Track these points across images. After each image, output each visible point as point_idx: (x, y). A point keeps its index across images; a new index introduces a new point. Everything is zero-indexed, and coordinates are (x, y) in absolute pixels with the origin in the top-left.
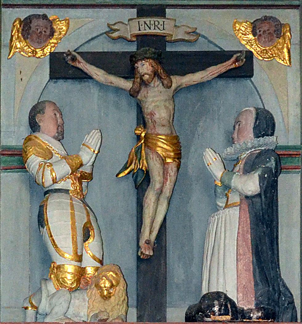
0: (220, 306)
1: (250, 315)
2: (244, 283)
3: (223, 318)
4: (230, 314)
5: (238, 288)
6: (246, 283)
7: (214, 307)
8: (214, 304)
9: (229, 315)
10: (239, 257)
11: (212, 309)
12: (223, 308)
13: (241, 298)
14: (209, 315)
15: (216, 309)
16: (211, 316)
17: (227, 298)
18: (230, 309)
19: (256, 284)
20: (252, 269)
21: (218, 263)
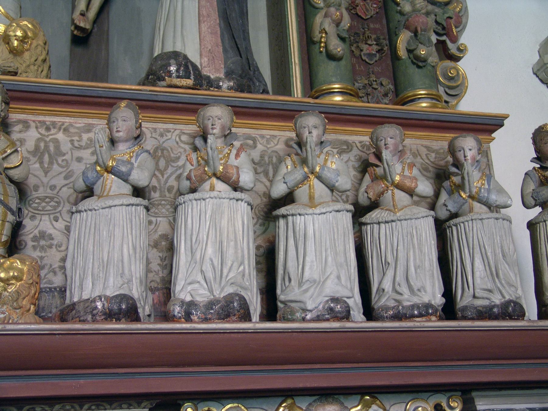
0: (179, 66)
1: (219, 83)
2: (210, 48)
3: (183, 82)
4: (192, 77)
5: (201, 52)
6: (212, 47)
7: (170, 66)
8: (170, 63)
9: (190, 79)
10: (201, 18)
11: (167, 68)
12: (182, 68)
13: (206, 64)
14: (162, 76)
15: (173, 68)
16: (166, 77)
17: (185, 57)
18: (192, 72)
19: (225, 51)
20: (219, 32)
21: (175, 27)
